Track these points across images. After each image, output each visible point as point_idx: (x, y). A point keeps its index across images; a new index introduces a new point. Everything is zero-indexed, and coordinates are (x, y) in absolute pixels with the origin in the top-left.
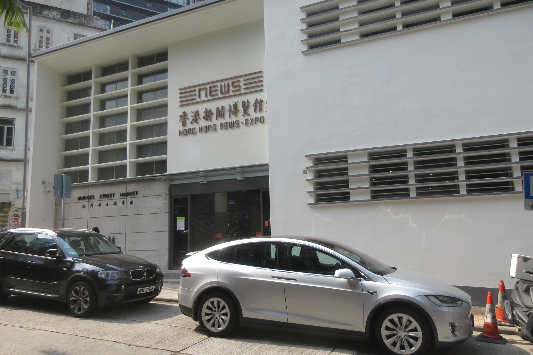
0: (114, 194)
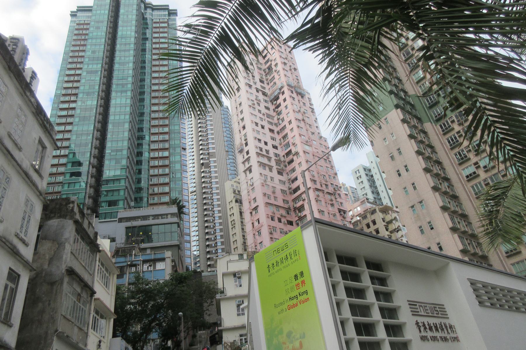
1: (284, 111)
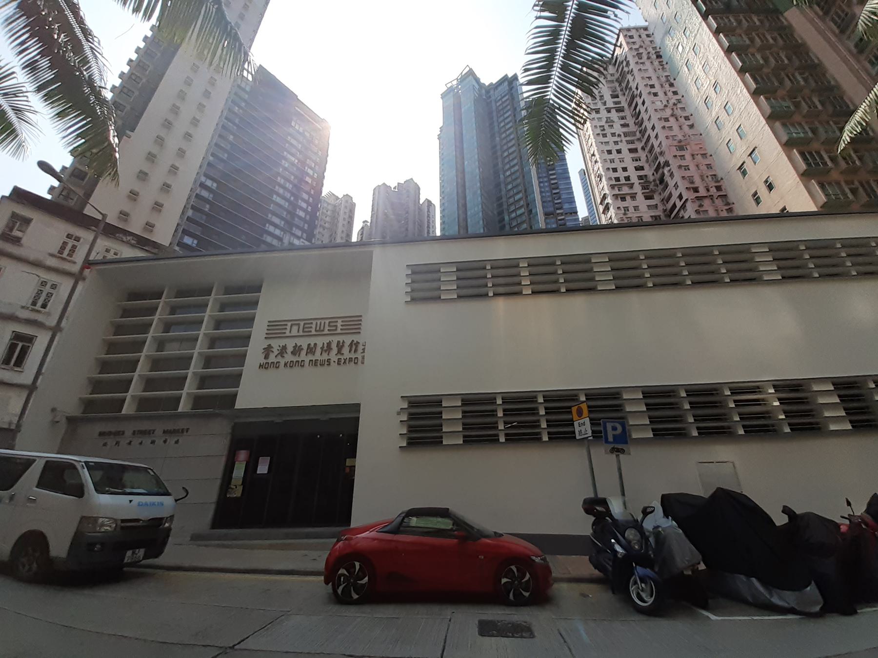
0: (154, 431)
1: (645, 117)
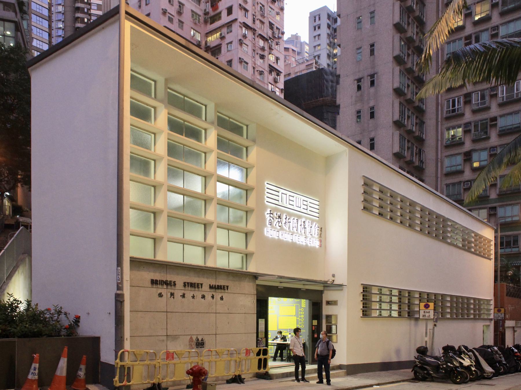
0: (202, 284)
